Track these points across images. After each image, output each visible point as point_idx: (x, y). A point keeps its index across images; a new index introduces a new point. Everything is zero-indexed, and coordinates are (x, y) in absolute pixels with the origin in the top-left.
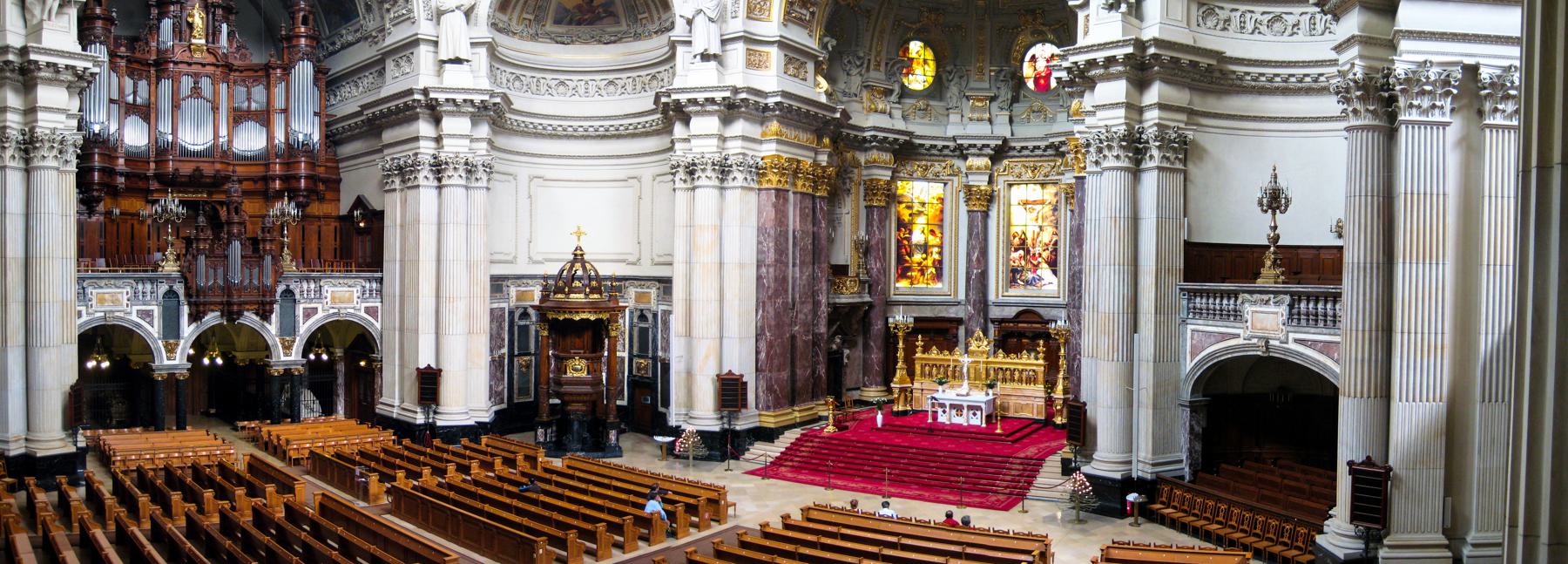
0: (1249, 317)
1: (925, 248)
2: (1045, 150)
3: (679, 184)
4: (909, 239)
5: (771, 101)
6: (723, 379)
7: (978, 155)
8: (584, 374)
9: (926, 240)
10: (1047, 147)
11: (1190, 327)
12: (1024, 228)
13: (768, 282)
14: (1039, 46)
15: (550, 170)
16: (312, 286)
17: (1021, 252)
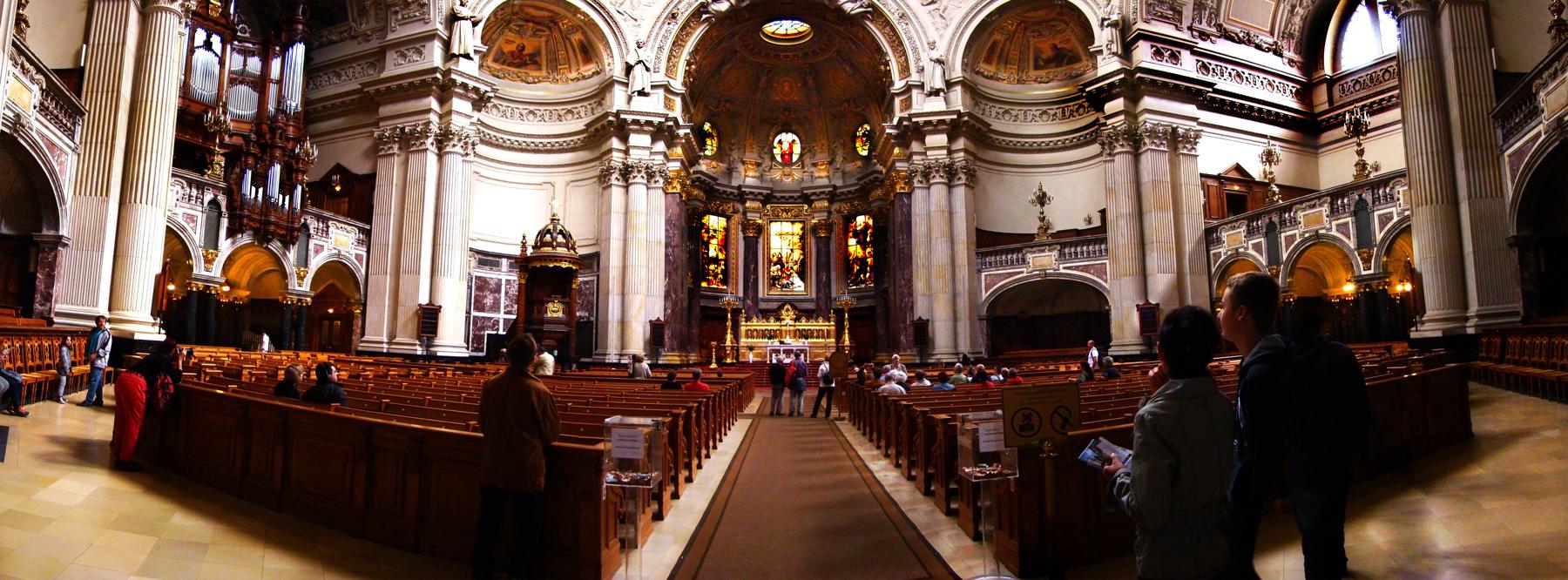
0: (1031, 261)
1: (716, 260)
2: (796, 199)
3: (614, 181)
4: (708, 254)
5: (681, 132)
6: (654, 324)
7: (753, 200)
8: (560, 314)
9: (717, 256)
10: (798, 197)
11: (983, 274)
12: (780, 251)
13: (673, 258)
14: (784, 134)
15: (485, 169)
16: (321, 225)
17: (779, 266)
